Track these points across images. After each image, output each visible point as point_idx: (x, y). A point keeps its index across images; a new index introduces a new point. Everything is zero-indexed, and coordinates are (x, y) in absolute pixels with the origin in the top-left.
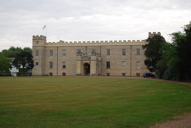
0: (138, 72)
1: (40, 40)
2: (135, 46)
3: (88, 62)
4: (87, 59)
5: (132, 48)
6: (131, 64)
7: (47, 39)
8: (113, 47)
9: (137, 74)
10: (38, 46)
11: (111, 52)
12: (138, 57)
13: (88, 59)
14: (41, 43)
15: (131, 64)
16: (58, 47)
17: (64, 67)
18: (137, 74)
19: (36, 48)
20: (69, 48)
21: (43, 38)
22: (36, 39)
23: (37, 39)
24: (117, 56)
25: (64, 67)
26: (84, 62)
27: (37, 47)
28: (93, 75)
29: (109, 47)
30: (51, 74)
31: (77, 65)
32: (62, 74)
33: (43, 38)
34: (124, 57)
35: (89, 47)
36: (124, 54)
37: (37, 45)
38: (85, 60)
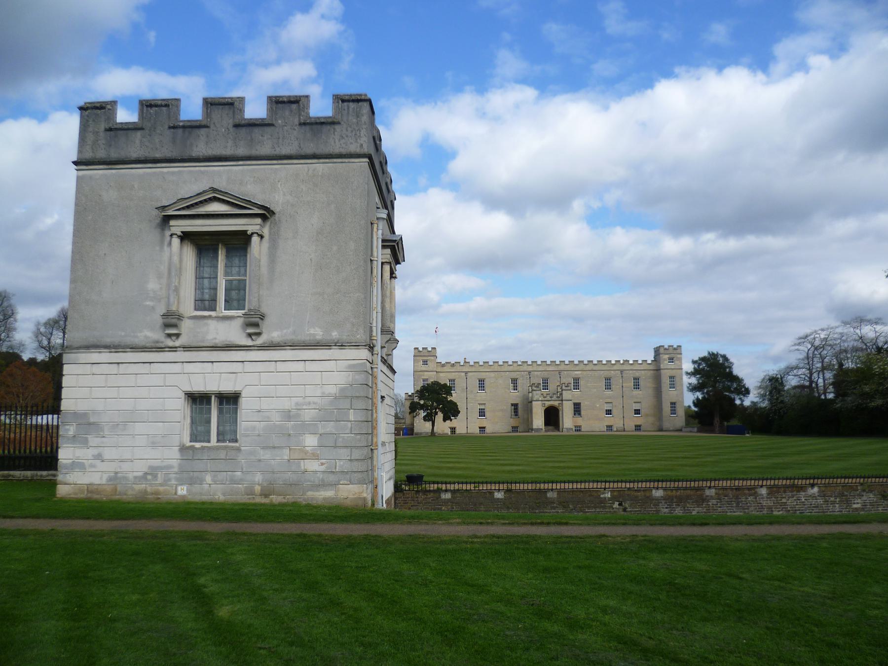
0: (638, 424)
3: (556, 403)
5: (624, 375)
7: (439, 352)
8: (585, 373)
10: (424, 369)
11: (582, 383)
12: (636, 392)
13: (555, 397)
14: (431, 366)
16: (466, 373)
17: (482, 413)
20: (492, 375)
21: (432, 352)
22: (422, 354)
23: (694, 362)
25: (482, 413)
26: (548, 404)
28: (569, 429)
30: (453, 430)
31: (534, 410)
32: (478, 431)
33: (432, 352)
34: (608, 392)
36: (608, 387)
37: (424, 368)
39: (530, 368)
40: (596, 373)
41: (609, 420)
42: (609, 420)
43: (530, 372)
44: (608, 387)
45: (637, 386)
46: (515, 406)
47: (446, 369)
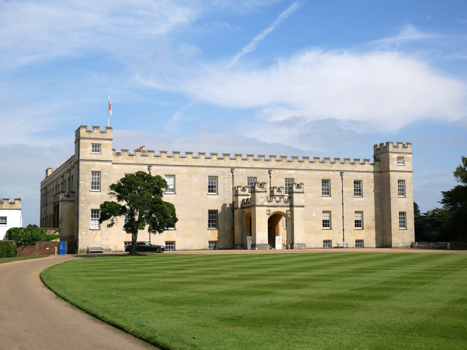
0: (360, 238)
1: (107, 142)
2: (352, 173)
4: (280, 204)
6: (343, 217)
8: (300, 172)
9: (357, 241)
15: (343, 217)
18: (357, 241)
19: (94, 166)
20: (185, 170)
24: (311, 195)
26: (273, 210)
27: (97, 163)
29: (293, 172)
34: (326, 199)
35: (240, 170)
38: (276, 204)
39: (233, 164)
40: (312, 173)
41: (327, 234)
42: (327, 234)
43: (232, 169)
44: (327, 192)
45: (358, 192)
46: (212, 213)
47: (121, 159)
